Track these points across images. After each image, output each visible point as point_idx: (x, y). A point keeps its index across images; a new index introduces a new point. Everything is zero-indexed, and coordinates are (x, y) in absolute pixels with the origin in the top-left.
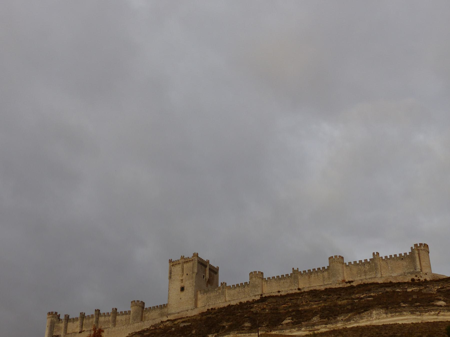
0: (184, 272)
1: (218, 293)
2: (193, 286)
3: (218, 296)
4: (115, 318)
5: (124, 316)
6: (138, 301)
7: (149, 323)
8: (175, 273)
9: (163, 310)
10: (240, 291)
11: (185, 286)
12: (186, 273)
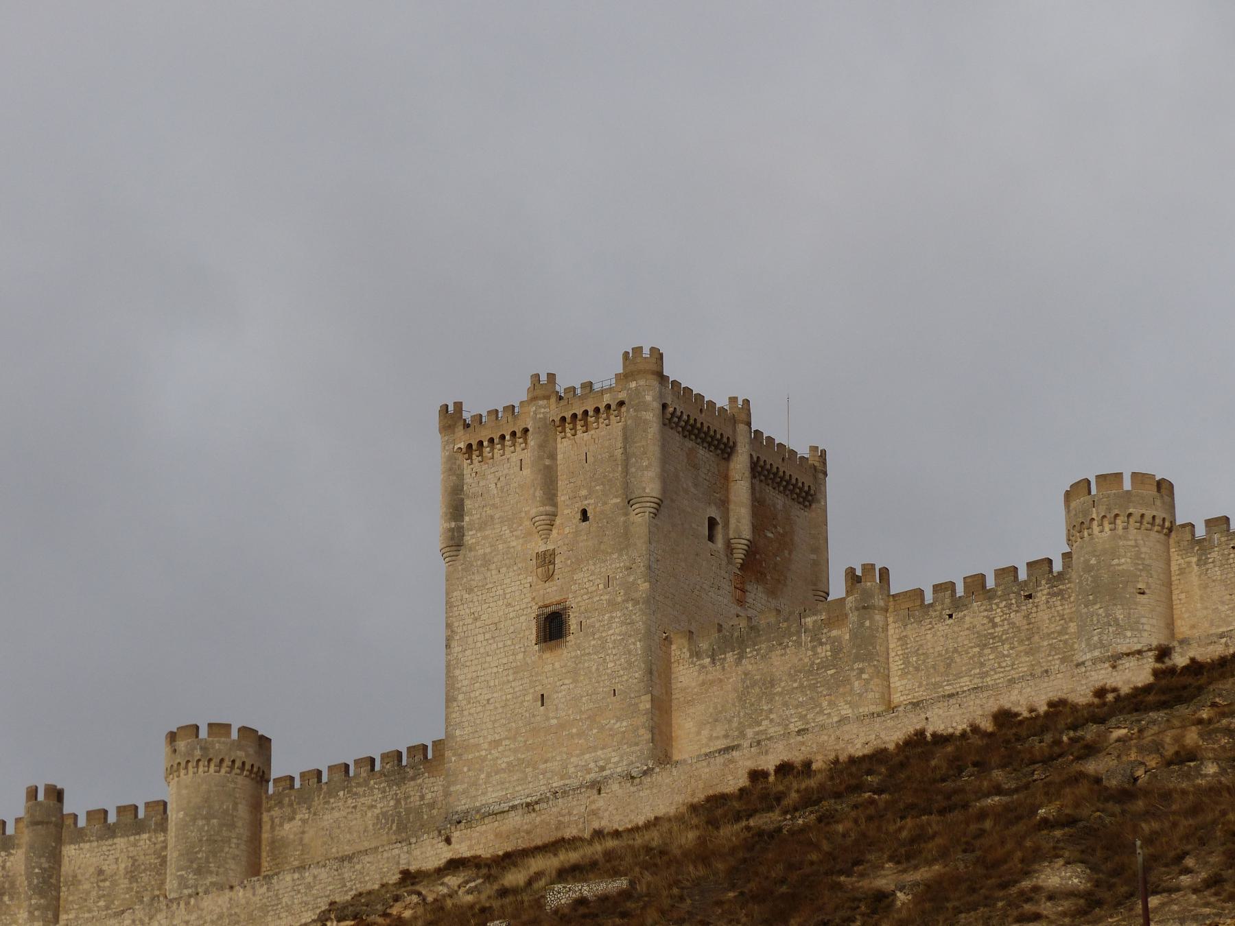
0: (562, 498)
1: (824, 651)
2: (636, 602)
3: (833, 671)
4: (55, 858)
5: (121, 842)
6: (218, 729)
7: (309, 887)
8: (494, 506)
10: (995, 625)
11: (571, 602)
12: (578, 506)
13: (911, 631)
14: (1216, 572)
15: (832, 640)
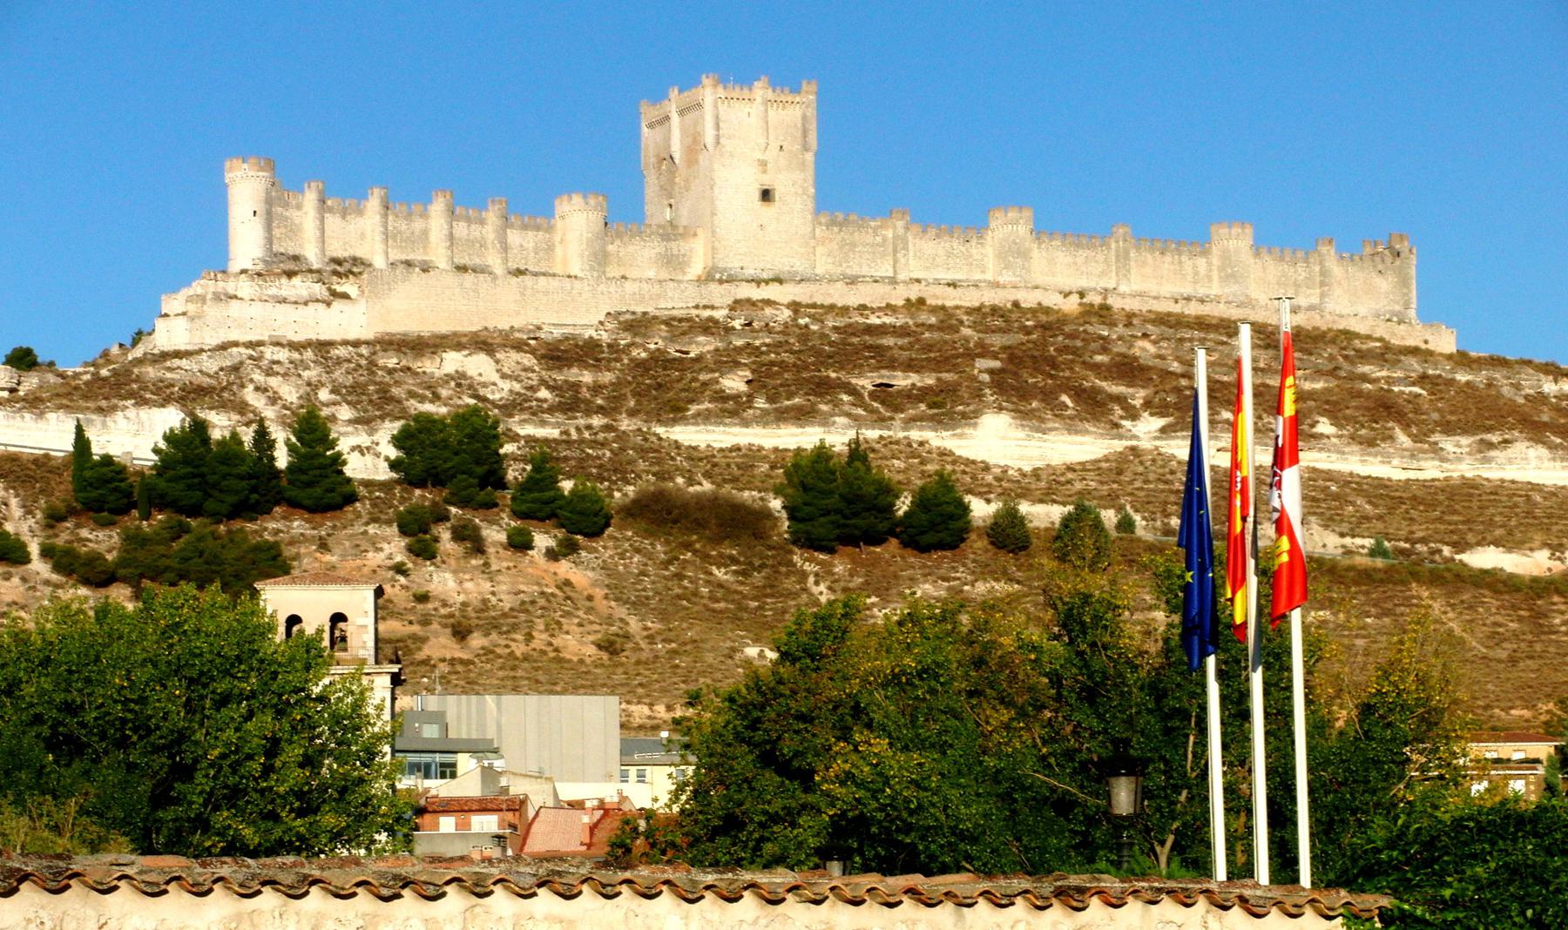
1: (879, 239)
9: (673, 245)
13: (917, 241)
14: (1044, 254)
15: (884, 236)
